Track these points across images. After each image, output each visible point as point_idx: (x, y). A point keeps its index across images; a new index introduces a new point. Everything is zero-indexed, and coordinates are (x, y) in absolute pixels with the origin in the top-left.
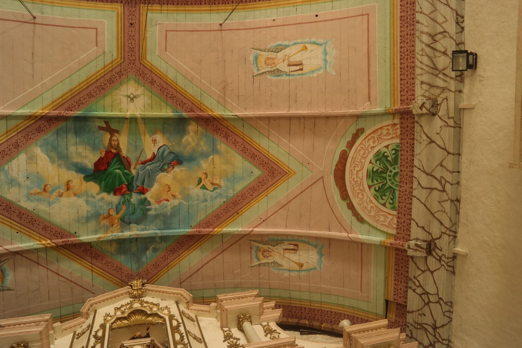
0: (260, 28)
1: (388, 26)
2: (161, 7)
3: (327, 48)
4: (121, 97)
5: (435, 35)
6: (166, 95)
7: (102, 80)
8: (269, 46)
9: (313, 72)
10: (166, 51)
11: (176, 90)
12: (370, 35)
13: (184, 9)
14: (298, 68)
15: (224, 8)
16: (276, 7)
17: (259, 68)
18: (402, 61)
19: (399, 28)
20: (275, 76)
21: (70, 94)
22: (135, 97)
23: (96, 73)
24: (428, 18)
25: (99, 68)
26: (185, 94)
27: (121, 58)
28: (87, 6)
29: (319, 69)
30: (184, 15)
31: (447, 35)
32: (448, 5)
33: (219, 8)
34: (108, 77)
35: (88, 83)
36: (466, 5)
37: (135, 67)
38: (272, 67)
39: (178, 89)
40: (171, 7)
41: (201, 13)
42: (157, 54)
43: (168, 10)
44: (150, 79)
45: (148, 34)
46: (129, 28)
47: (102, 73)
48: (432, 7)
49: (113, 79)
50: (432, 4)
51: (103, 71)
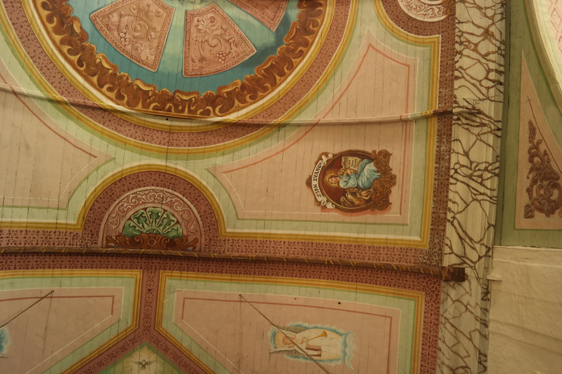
0: (281, 304)
1: (410, 338)
2: (181, 273)
3: (347, 340)
4: (133, 364)
5: (457, 369)
6: (179, 363)
7: (115, 348)
8: (288, 325)
9: (331, 360)
10: (182, 318)
11: (190, 359)
12: (392, 340)
13: (204, 276)
14: (316, 353)
15: (245, 278)
16: (299, 285)
17: (277, 346)
18: (424, 347)
19: (421, 345)
20: (292, 357)
21: (80, 364)
22: (147, 363)
23: (109, 341)
24: (449, 351)
25: (112, 337)
26: (198, 363)
27: (136, 325)
28: (106, 274)
29: (337, 360)
30: (203, 283)
31: (469, 371)
32: (471, 339)
33: (241, 278)
34: (120, 345)
35: (99, 352)
36: (490, 346)
37: (149, 333)
38: (290, 347)
39: (192, 358)
40: (191, 274)
41: (221, 282)
42: (173, 321)
43: (187, 277)
44: (164, 346)
45: (166, 301)
46: (147, 294)
47: (114, 342)
48: (455, 340)
49: (126, 347)
50: (455, 337)
51: (116, 339)
